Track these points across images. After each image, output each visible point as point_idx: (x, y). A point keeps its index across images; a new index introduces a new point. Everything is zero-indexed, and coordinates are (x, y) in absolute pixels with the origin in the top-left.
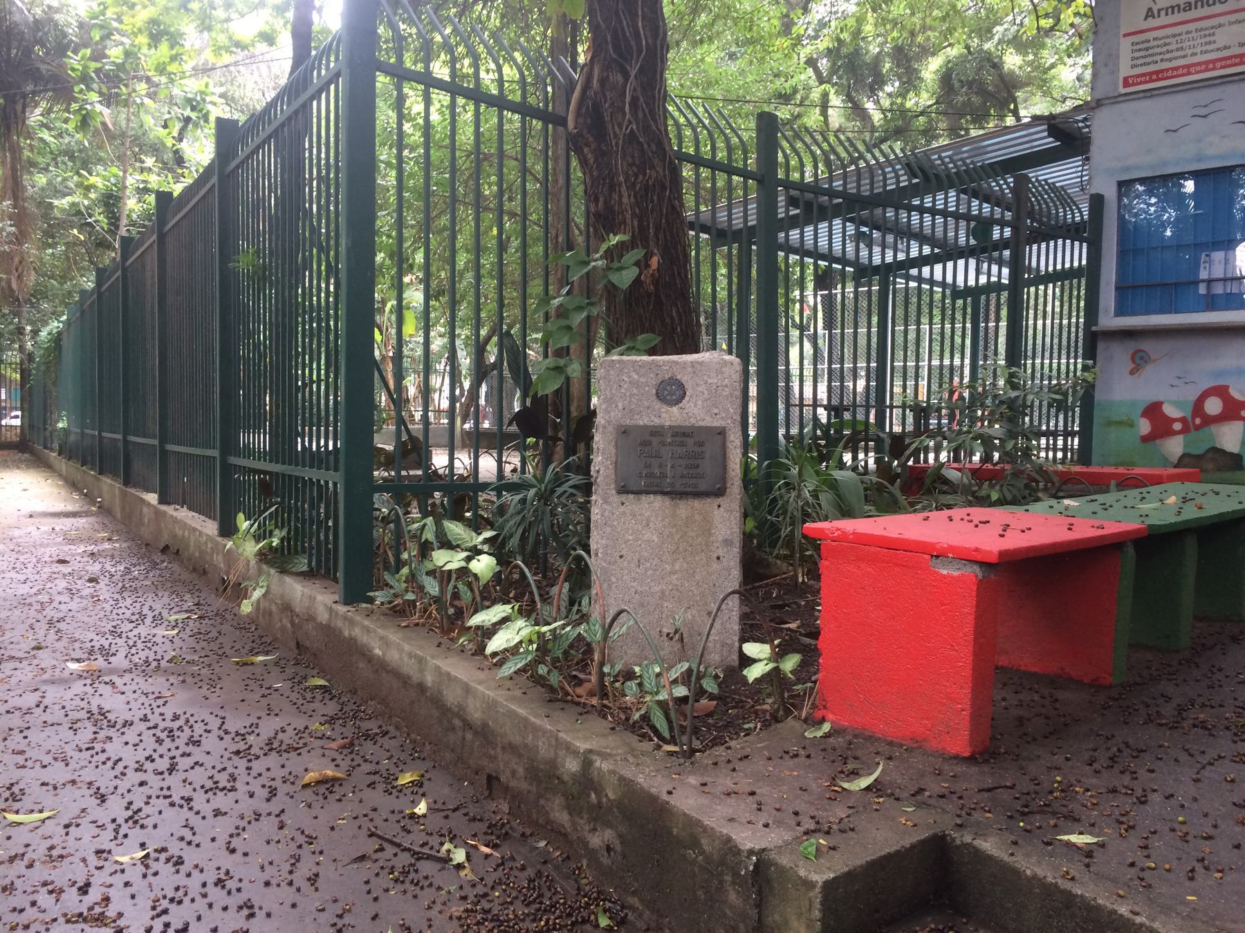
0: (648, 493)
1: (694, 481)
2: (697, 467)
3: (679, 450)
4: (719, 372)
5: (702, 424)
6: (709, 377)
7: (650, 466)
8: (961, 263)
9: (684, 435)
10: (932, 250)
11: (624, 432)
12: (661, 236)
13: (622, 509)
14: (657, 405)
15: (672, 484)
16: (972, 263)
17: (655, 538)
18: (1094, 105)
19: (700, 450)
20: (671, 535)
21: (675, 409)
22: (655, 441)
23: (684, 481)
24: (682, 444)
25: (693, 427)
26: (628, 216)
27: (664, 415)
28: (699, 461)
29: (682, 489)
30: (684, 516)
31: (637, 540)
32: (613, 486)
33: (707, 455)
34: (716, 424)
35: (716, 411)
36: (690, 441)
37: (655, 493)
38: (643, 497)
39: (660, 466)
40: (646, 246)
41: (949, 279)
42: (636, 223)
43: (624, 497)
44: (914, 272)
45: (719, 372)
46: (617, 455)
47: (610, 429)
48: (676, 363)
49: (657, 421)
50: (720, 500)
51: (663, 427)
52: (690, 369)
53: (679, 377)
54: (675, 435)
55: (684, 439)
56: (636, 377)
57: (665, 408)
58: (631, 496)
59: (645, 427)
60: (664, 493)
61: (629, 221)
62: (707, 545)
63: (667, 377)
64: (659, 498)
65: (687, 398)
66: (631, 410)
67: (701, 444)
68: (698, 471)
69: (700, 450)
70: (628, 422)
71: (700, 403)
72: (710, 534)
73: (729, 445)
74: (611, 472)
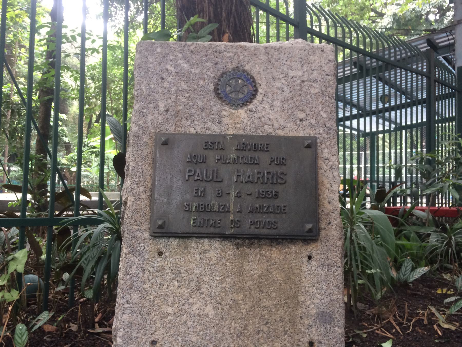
0: (200, 236)
1: (271, 218)
2: (276, 196)
3: (249, 171)
4: (304, 61)
5: (280, 133)
6: (290, 68)
7: (203, 195)
8: (368, 119)
9: (256, 148)
10: (358, 112)
11: (165, 143)
12: (232, 20)
13: (159, 262)
14: (216, 105)
15: (237, 224)
16: (374, 119)
17: (209, 310)
18: (456, 23)
19: (279, 170)
20: (235, 305)
21: (242, 113)
22: (212, 156)
23: (258, 218)
24: (254, 163)
25: (269, 137)
26: (206, 5)
27: (225, 121)
28: (279, 188)
29: (253, 230)
30: (255, 273)
31: (180, 313)
32: (146, 226)
33: (290, 179)
34: (301, 134)
35: (302, 115)
36: (265, 158)
37: (211, 236)
38: (193, 243)
39: (219, 196)
40: (220, 22)
41: (362, 128)
42: (211, 9)
43: (162, 244)
44: (348, 123)
45: (304, 61)
46: (153, 178)
47: (145, 139)
48: (244, 48)
49: (216, 129)
50: (311, 249)
51: (224, 136)
52: (263, 57)
53: (247, 68)
54: (242, 148)
55: (256, 155)
56: (186, 66)
57: (227, 111)
58: (174, 242)
59: (197, 134)
60: (224, 237)
61: (206, 9)
62: (293, 323)
63: (230, 67)
64: (217, 244)
65: (259, 97)
66: (177, 114)
67: (281, 162)
68: (276, 202)
69: (279, 170)
70: (172, 129)
71: (278, 103)
72: (298, 304)
73: (322, 164)
74: (144, 204)
